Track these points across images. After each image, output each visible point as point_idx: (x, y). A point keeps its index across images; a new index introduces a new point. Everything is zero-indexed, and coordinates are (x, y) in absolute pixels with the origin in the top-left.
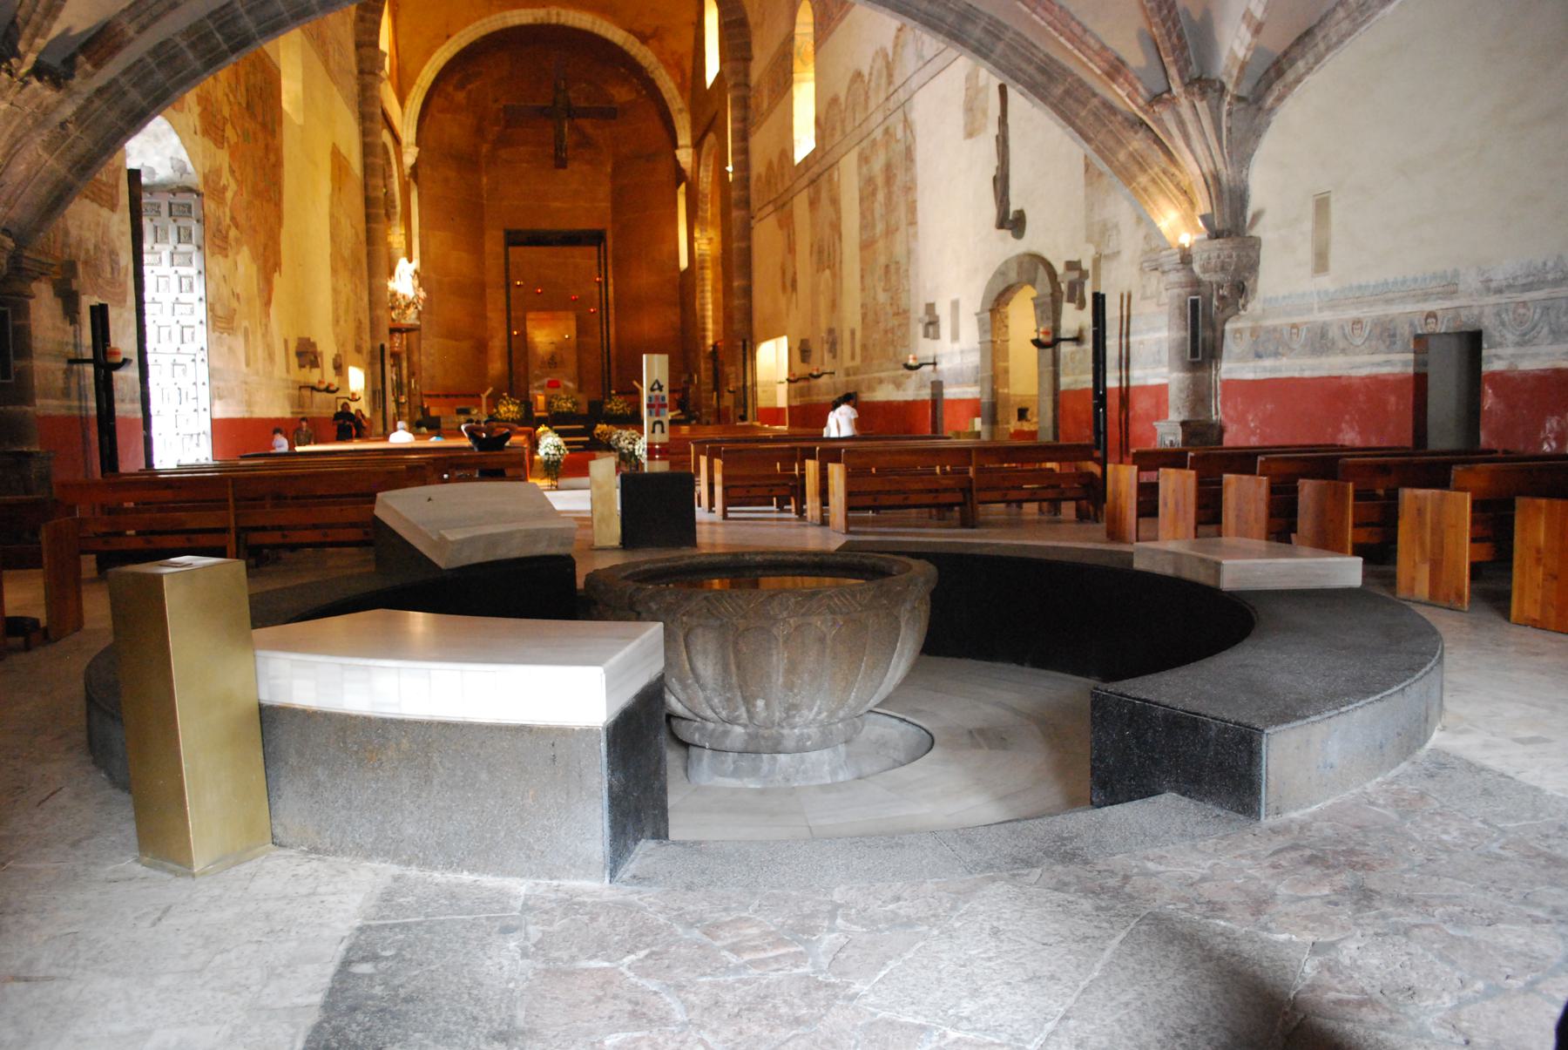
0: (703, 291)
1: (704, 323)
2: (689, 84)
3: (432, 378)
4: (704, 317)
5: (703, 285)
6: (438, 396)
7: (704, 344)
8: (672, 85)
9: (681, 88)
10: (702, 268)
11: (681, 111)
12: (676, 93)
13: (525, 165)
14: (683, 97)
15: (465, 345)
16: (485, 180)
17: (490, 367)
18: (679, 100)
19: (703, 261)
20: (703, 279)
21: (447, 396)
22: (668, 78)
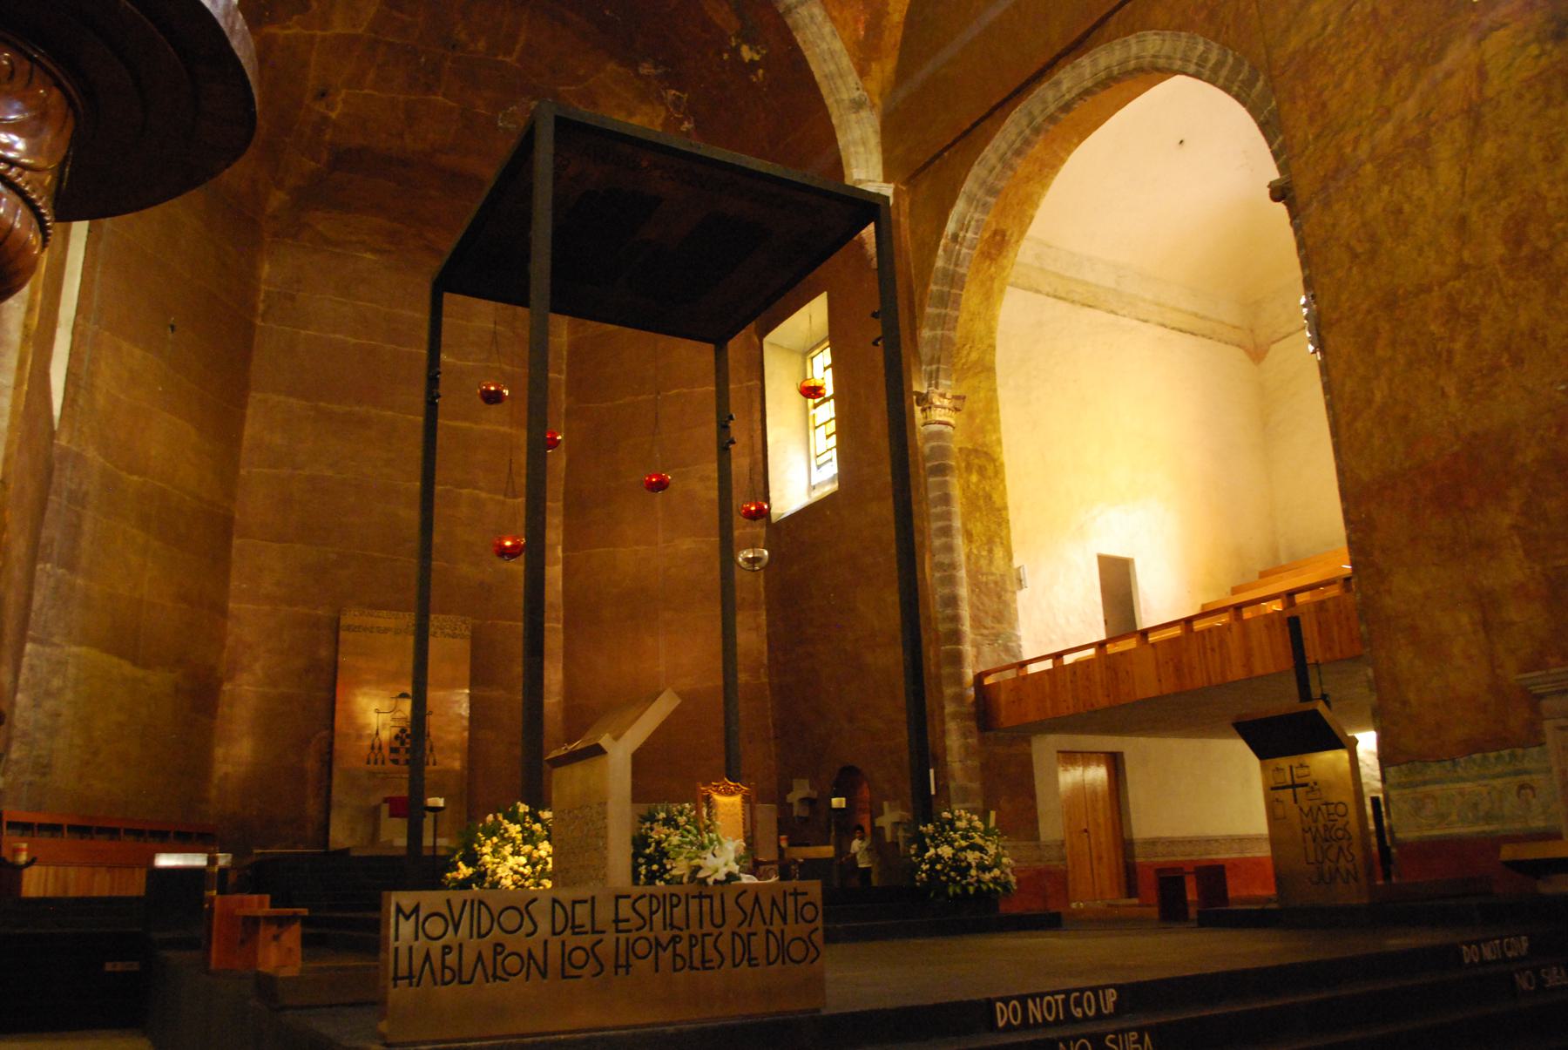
0: (946, 531)
1: (956, 619)
2: (893, 35)
3: (44, 768)
4: (952, 601)
5: (947, 516)
6: (54, 829)
7: (958, 679)
8: (838, 45)
9: (865, 54)
10: (942, 470)
11: (857, 105)
12: (846, 62)
13: (369, 256)
14: (863, 73)
15: (160, 680)
16: (266, 269)
17: (219, 752)
18: (853, 78)
19: (943, 452)
20: (946, 499)
21: (81, 830)
22: (828, 28)
